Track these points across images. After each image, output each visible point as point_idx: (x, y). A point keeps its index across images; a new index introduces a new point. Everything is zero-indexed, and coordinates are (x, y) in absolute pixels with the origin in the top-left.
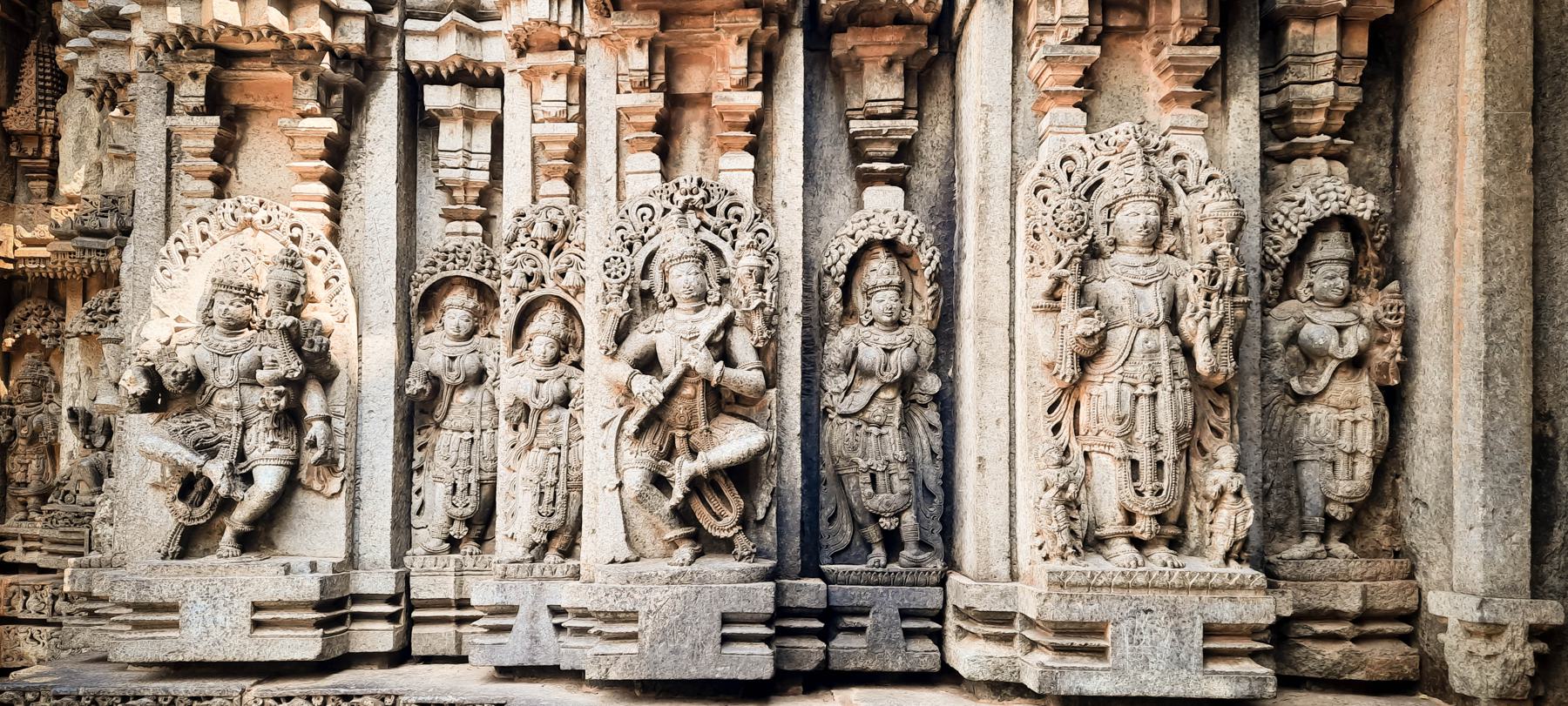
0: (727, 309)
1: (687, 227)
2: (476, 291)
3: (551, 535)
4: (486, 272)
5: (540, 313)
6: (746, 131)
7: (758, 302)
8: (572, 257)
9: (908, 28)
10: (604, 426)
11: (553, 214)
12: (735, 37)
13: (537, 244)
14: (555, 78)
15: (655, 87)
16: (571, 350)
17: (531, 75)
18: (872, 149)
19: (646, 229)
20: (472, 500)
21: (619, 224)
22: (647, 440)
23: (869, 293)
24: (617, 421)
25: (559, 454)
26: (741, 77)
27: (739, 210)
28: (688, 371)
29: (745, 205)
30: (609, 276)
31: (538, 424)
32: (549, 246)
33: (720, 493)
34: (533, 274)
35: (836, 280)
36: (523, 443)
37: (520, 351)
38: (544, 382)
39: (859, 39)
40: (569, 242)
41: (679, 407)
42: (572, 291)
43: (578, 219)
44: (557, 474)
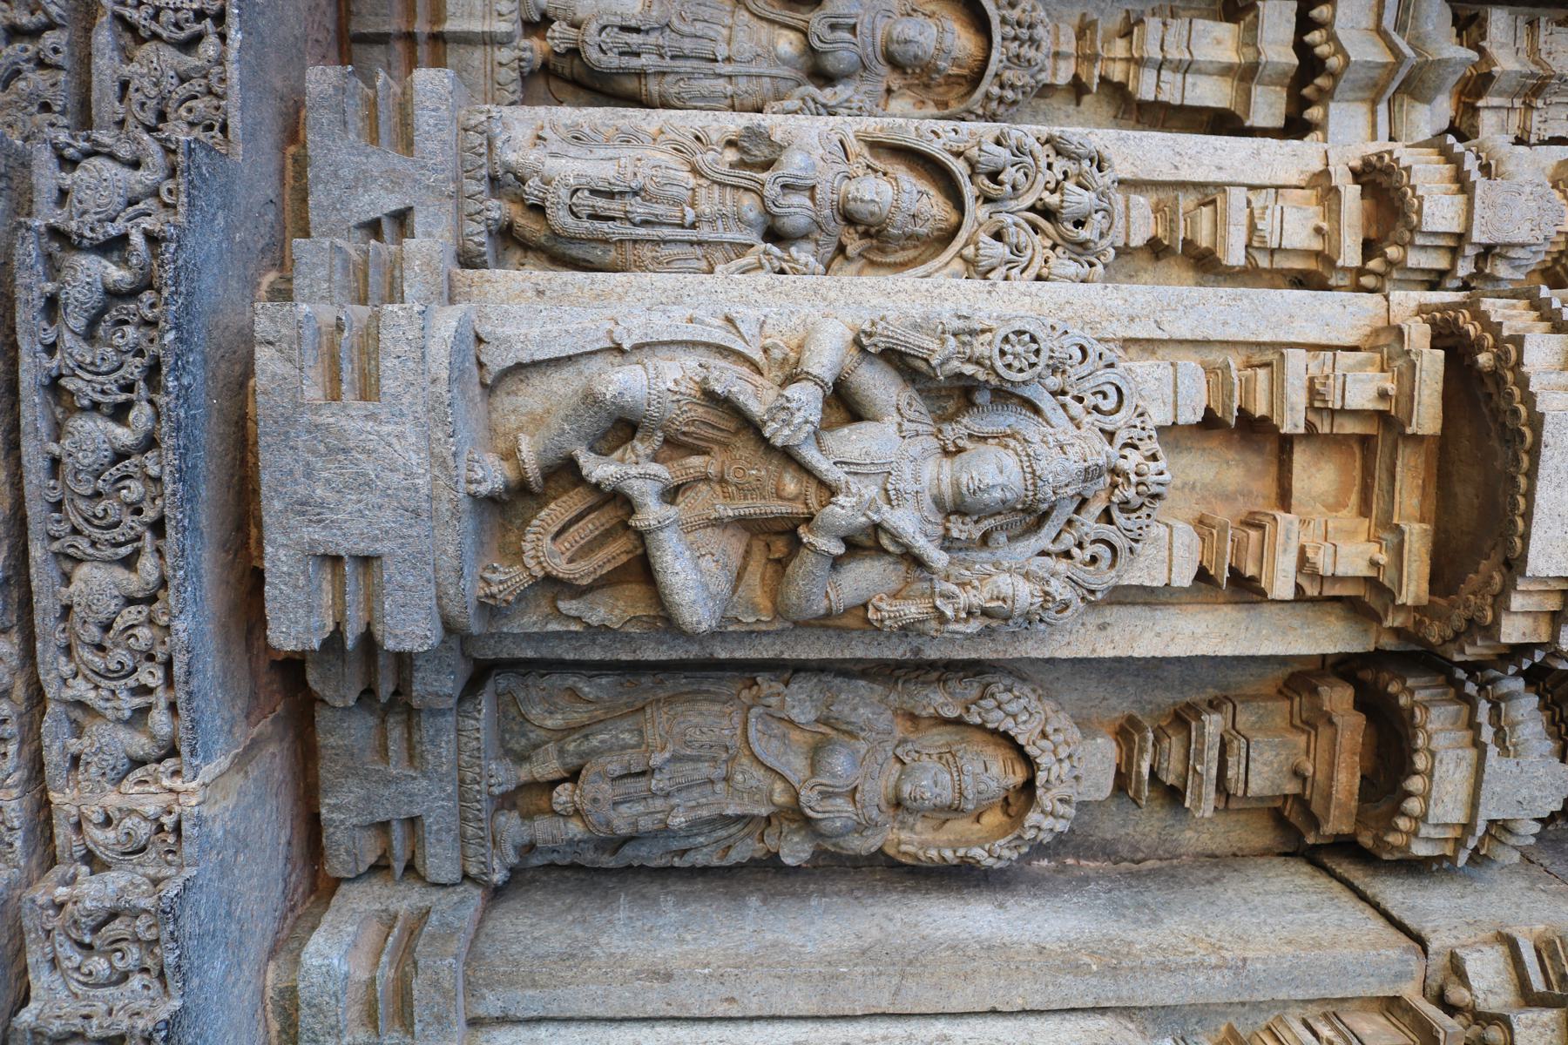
0: (938, 558)
1: (1085, 481)
2: (965, 72)
3: (539, 210)
4: (995, 90)
5: (932, 192)
6: (1230, 567)
7: (949, 613)
8: (1029, 252)
9: (1354, 804)
10: (729, 320)
11: (1097, 221)
12: (1383, 559)
13: (1053, 192)
14: (1318, 231)
15: (1313, 418)
16: (865, 242)
17: (1322, 185)
18: (1174, 744)
19: (1080, 400)
20: (612, 61)
21: (1090, 351)
22: (700, 410)
23: (948, 757)
24: (739, 345)
25: (682, 226)
26: (1320, 566)
27: (1104, 564)
28: (829, 490)
29: (1113, 573)
30: (1006, 339)
31: (737, 187)
32: (1048, 213)
33: (606, 536)
34: (1001, 184)
35: (973, 708)
36: (705, 159)
37: (866, 152)
38: (812, 198)
39: (1348, 734)
40: (1054, 247)
41: (759, 470)
42: (969, 252)
43: (1091, 265)
44: (645, 223)
